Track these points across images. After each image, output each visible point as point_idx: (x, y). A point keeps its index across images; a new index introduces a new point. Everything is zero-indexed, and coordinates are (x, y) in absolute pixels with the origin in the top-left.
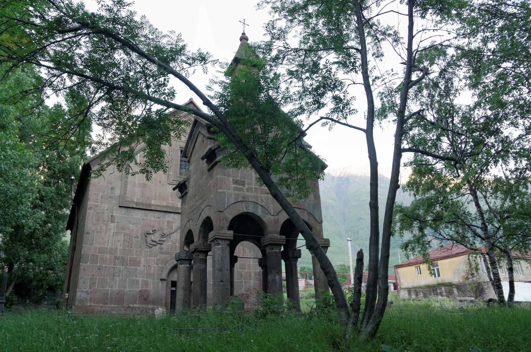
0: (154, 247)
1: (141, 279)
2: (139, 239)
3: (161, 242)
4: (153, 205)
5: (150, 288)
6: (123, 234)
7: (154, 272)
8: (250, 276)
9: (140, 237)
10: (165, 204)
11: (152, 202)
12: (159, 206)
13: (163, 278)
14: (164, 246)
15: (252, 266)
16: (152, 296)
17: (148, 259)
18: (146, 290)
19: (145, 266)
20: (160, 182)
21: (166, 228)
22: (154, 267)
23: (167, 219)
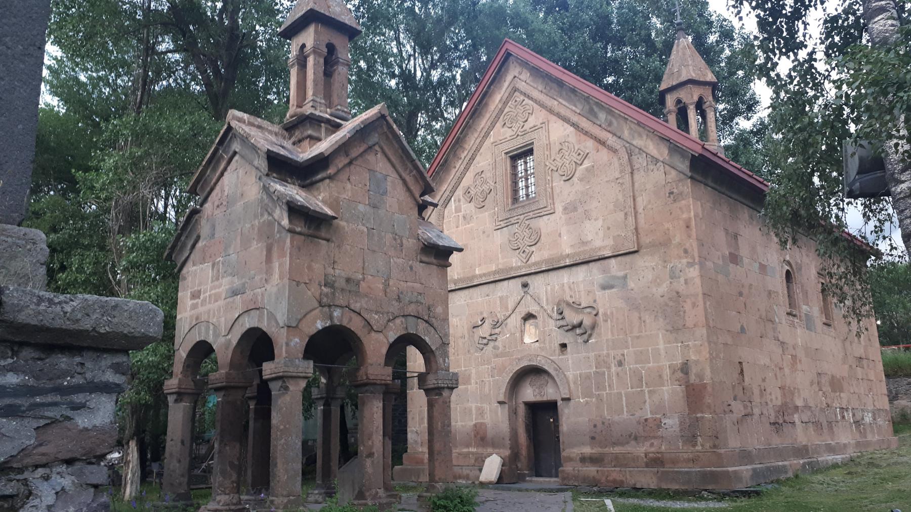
1: (473, 406)
3: (494, 337)
5: (488, 420)
7: (490, 390)
8: (660, 376)
9: (467, 336)
11: (477, 272)
12: (484, 275)
14: (499, 343)
15: (663, 352)
16: (490, 434)
18: (482, 423)
20: (484, 232)
23: (499, 294)
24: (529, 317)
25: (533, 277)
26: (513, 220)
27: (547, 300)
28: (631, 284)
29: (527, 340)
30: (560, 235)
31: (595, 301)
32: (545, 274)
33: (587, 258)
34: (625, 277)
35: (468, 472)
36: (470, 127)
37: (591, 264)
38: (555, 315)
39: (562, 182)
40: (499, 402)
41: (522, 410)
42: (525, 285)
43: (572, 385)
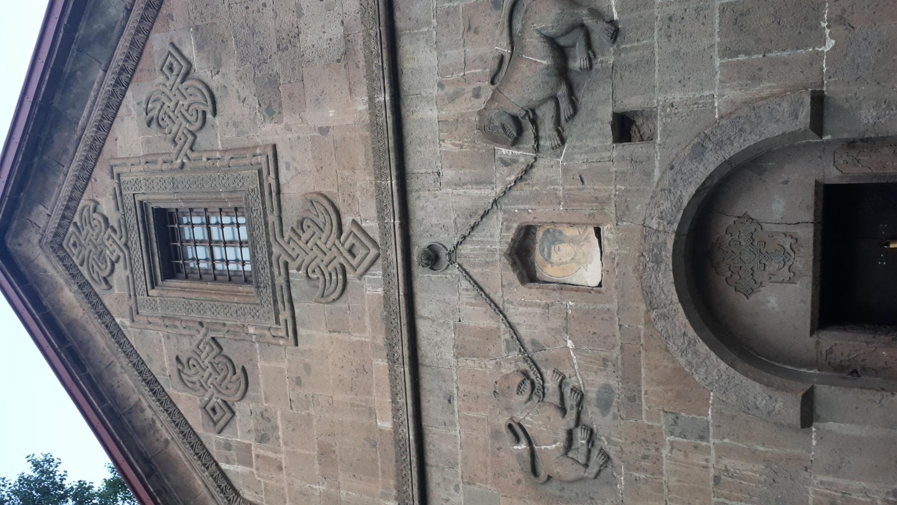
0: (603, 442)
3: (571, 401)
4: (396, 426)
7: (753, 456)
11: (387, 425)
13: (794, 414)
14: (593, 383)
17: (673, 481)
21: (491, 364)
22: (722, 452)
23: (449, 355)
24: (522, 255)
25: (416, 229)
26: (280, 281)
27: (478, 183)
29: (590, 274)
30: (324, 131)
32: (413, 184)
33: (378, 29)
36: (100, 376)
37: (401, 23)
38: (522, 154)
39: (217, 120)
40: (808, 418)
41: (843, 343)
42: (433, 258)
43: (764, 88)
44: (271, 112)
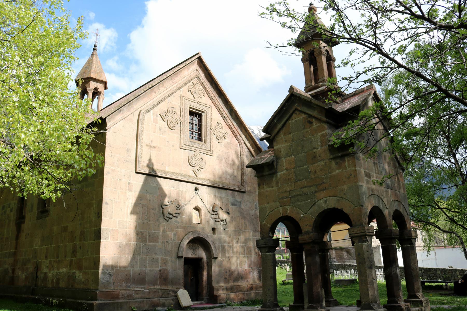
0: (170, 220)
2: (156, 211)
3: (177, 215)
4: (167, 172)
5: (169, 267)
6: (141, 205)
7: (172, 248)
10: (178, 172)
11: (167, 169)
16: (171, 276)
18: (165, 270)
19: (163, 243)
20: (173, 146)
28: (243, 207)
31: (229, 210)
34: (240, 202)
35: (164, 301)
44: (218, 157)
